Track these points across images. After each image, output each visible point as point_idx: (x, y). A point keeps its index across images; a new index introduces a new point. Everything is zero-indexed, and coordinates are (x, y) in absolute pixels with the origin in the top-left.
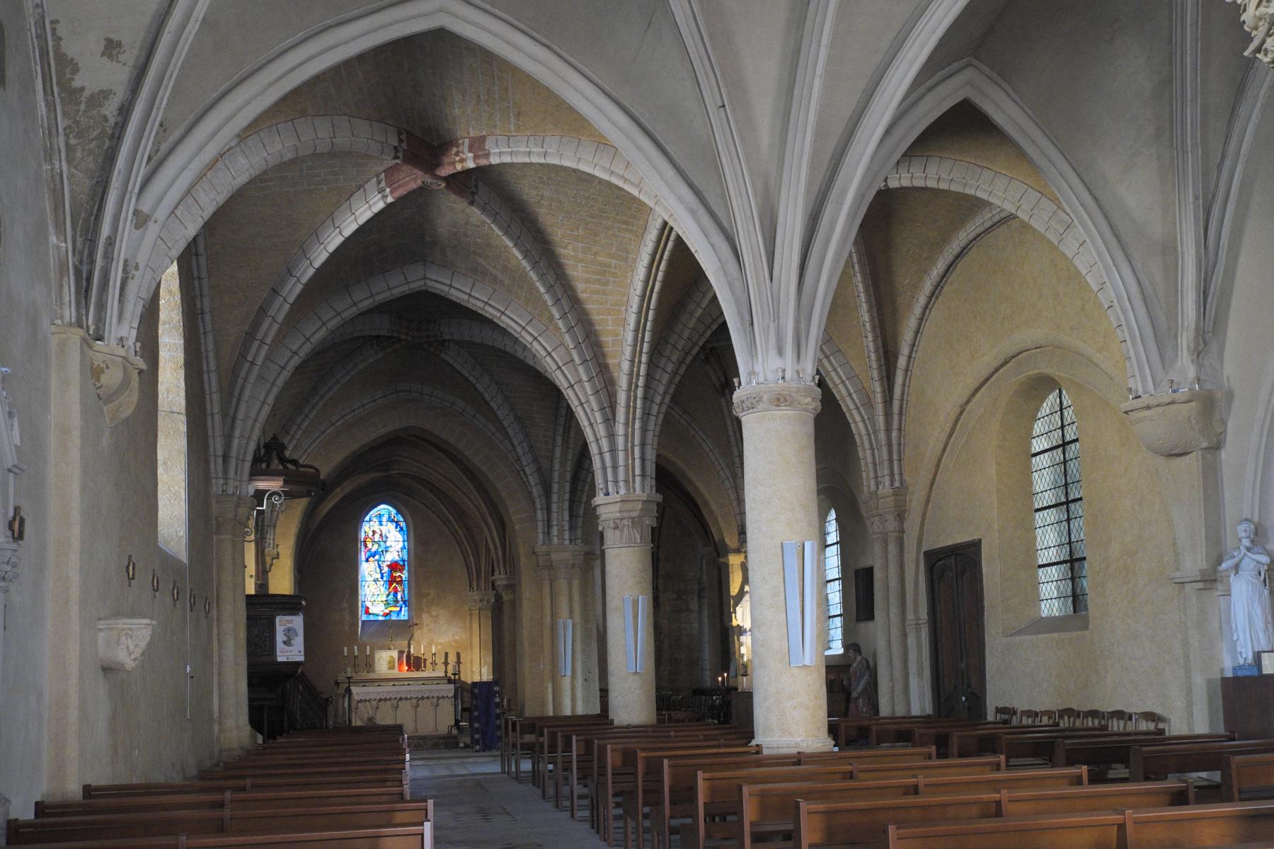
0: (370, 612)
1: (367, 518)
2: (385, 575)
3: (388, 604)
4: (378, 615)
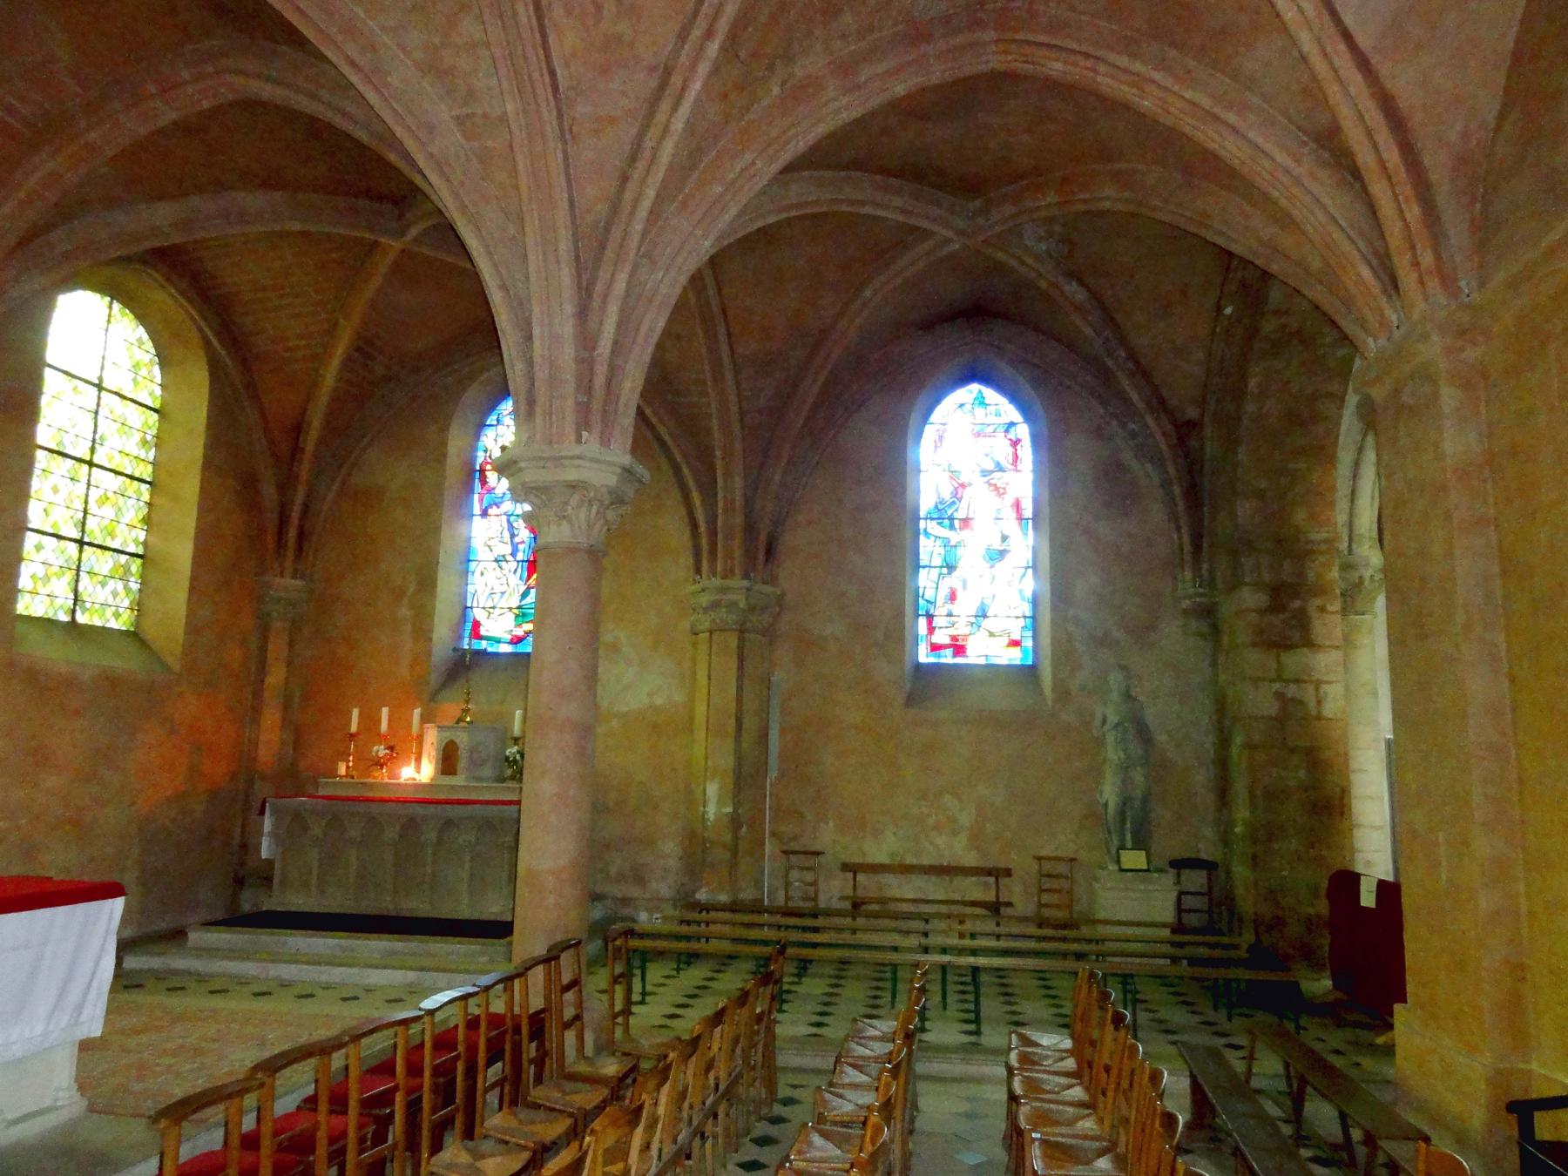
0: (483, 632)
1: (492, 420)
2: (521, 547)
3: (524, 615)
4: (498, 641)
